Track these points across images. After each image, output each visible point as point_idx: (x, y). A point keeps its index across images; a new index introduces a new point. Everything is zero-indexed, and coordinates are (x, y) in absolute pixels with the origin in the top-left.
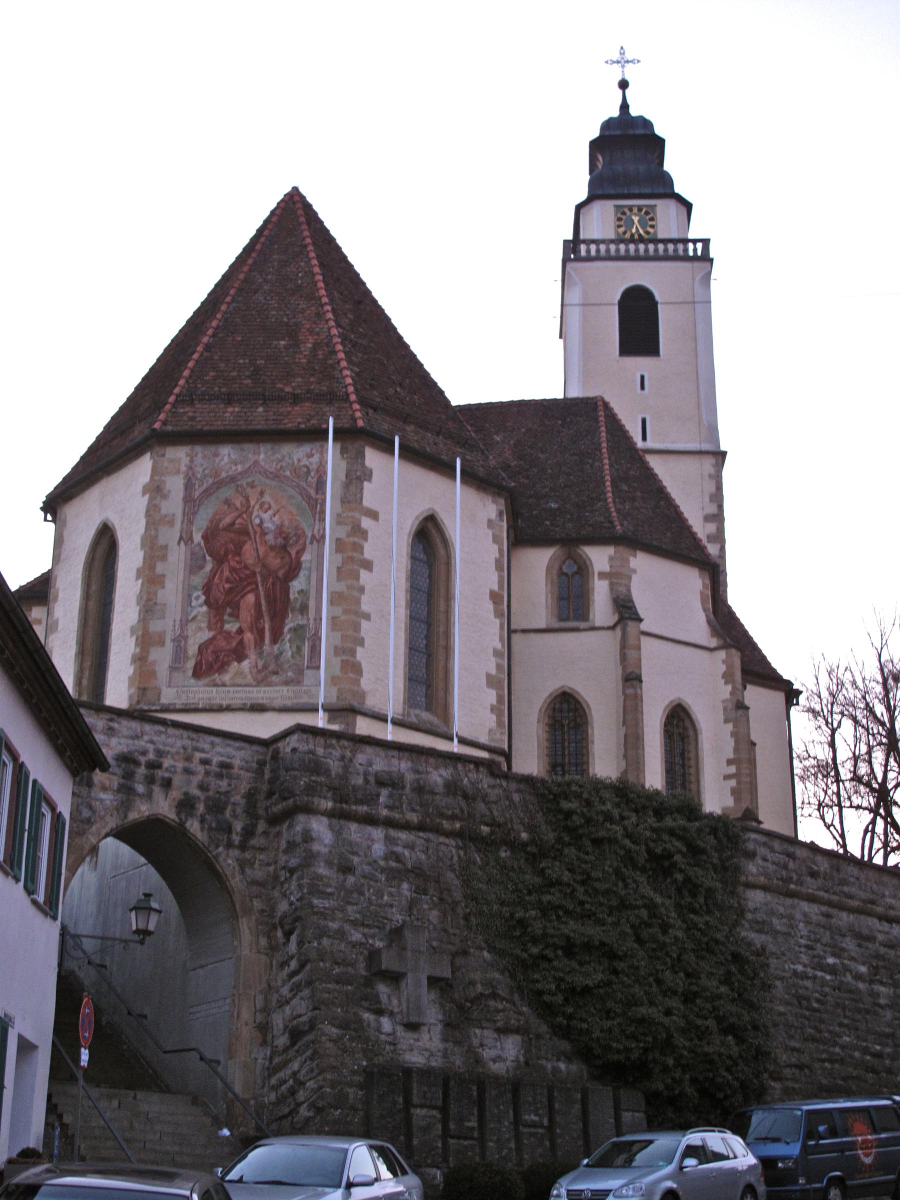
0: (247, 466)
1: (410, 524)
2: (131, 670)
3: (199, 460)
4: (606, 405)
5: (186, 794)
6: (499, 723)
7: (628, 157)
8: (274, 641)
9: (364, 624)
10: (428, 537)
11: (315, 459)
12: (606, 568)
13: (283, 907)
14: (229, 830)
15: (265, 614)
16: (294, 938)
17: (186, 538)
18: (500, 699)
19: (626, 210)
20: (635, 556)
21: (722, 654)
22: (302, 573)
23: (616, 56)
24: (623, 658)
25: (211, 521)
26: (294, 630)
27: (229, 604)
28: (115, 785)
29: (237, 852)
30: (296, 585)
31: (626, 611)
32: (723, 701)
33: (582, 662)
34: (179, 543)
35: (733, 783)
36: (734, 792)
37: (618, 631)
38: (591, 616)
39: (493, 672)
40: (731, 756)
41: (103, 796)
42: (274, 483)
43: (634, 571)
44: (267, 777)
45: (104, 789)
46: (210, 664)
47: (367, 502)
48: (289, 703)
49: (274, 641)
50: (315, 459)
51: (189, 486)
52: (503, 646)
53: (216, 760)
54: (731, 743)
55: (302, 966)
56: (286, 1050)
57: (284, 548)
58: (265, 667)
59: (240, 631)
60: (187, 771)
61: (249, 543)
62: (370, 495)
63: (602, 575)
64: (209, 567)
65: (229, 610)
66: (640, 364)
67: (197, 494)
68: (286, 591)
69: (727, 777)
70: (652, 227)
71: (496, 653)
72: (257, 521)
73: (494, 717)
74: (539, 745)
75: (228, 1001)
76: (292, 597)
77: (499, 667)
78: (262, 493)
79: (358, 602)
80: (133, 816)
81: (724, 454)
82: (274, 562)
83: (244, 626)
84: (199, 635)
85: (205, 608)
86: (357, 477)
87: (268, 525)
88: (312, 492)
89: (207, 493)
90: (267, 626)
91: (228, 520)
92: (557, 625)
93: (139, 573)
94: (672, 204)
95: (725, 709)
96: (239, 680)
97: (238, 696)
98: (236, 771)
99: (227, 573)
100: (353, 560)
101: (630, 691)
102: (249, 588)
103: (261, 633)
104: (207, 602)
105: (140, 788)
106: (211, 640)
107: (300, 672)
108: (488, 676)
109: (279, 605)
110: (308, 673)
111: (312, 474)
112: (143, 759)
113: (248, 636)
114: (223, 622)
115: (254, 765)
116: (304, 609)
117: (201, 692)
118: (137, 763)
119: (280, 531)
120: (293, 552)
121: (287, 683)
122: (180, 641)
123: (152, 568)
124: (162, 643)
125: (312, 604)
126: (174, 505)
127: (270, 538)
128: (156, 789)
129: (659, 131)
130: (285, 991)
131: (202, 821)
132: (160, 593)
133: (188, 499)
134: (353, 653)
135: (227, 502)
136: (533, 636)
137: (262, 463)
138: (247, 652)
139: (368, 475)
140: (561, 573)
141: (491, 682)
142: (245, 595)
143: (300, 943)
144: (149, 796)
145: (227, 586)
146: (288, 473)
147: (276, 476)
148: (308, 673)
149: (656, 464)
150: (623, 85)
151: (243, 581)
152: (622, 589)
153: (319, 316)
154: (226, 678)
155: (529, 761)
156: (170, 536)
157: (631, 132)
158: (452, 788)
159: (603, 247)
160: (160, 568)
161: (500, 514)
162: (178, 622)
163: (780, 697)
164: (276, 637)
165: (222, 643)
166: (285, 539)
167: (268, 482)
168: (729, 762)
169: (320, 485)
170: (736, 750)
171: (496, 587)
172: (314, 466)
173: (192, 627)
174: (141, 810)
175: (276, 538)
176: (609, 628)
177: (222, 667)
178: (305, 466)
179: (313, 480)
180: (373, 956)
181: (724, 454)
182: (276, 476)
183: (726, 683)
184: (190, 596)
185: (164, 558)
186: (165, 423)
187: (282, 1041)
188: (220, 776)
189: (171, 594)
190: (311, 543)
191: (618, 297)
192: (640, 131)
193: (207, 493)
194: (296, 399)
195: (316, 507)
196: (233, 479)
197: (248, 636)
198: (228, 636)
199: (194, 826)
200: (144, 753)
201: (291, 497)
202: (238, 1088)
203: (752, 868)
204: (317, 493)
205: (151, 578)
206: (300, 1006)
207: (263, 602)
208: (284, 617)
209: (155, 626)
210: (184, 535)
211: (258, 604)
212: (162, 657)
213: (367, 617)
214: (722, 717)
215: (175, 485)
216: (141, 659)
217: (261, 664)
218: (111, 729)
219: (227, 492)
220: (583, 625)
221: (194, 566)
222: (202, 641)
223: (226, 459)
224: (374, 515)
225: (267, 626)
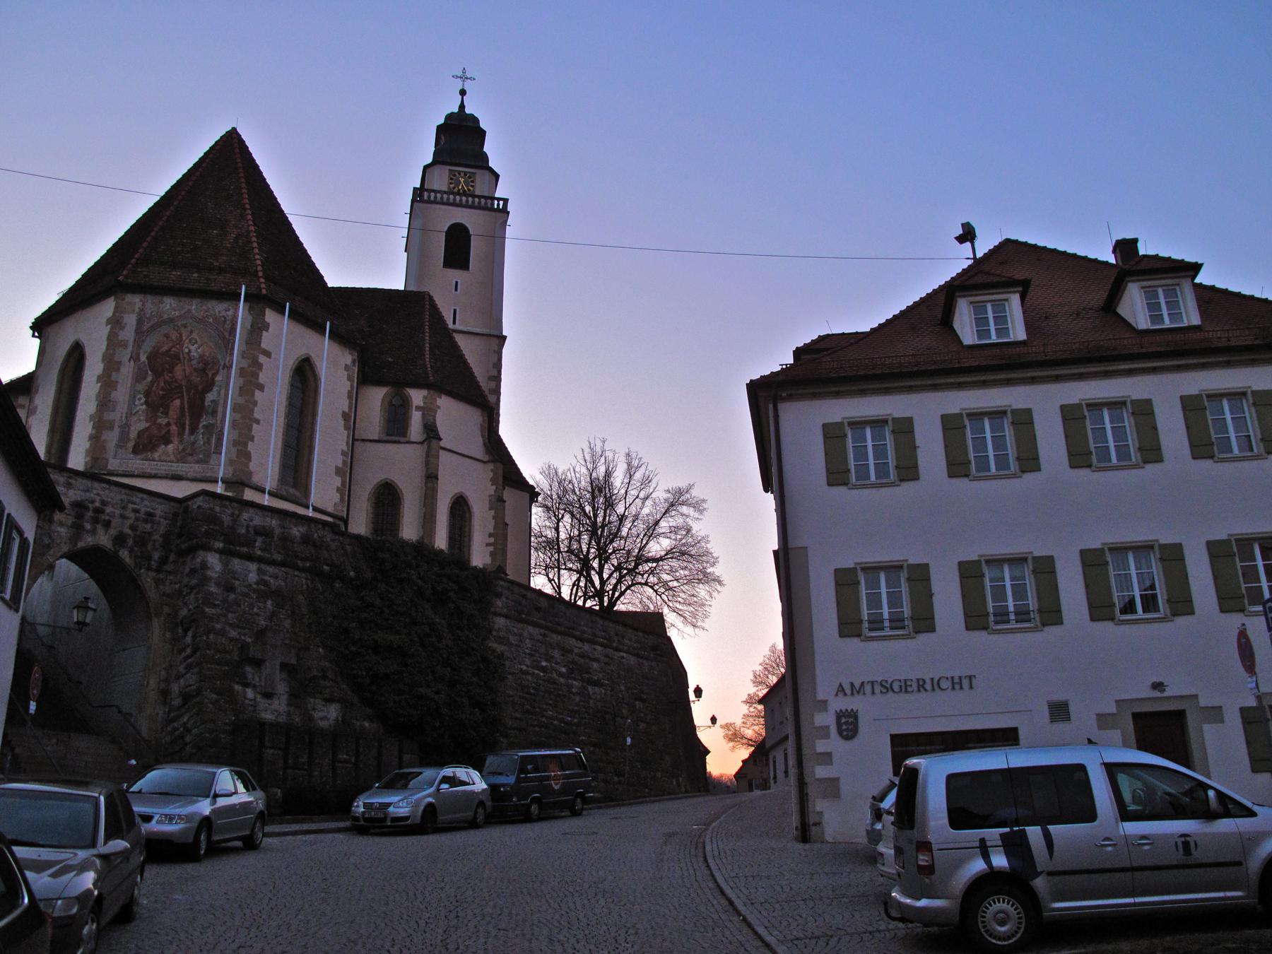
1: (291, 363)
2: (88, 445)
3: (149, 305)
4: (431, 298)
5: (121, 532)
6: (342, 500)
7: (460, 140)
8: (192, 431)
9: (255, 426)
10: (304, 373)
11: (230, 313)
12: (421, 404)
13: (184, 612)
14: (149, 558)
16: (190, 634)
17: (135, 358)
18: (343, 484)
21: (491, 466)
22: (215, 389)
23: (460, 74)
24: (427, 463)
28: (69, 522)
29: (154, 574)
30: (210, 397)
31: (431, 432)
33: (400, 464)
35: (491, 548)
36: (492, 554)
37: (425, 445)
41: (59, 529)
45: (61, 524)
46: (145, 445)
48: (198, 476)
49: (192, 431)
50: (230, 313)
51: (140, 322)
53: (143, 510)
54: (493, 522)
55: (194, 652)
56: (179, 708)
57: (204, 370)
58: (184, 450)
59: (168, 424)
60: (122, 516)
62: (267, 340)
63: (418, 408)
64: (149, 379)
66: (455, 275)
68: (203, 400)
69: (488, 545)
71: (344, 453)
77: (344, 463)
78: (191, 332)
79: (252, 411)
80: (81, 545)
81: (505, 338)
82: (196, 379)
84: (138, 425)
86: (258, 328)
87: (194, 354)
89: (153, 328)
91: (165, 348)
92: (386, 438)
93: (99, 379)
94: (487, 173)
96: (163, 457)
97: (163, 468)
99: (162, 384)
100: (251, 382)
103: (182, 427)
104: (146, 403)
105: (88, 526)
106: (147, 429)
107: (209, 456)
108: (337, 468)
110: (214, 456)
113: (174, 428)
114: (157, 417)
116: (214, 413)
117: (137, 464)
118: (87, 509)
119: (201, 356)
121: (197, 462)
122: (125, 427)
123: (109, 376)
124: (111, 428)
125: (220, 410)
126: (128, 334)
127: (194, 362)
128: (99, 527)
130: (182, 669)
131: (131, 551)
132: (113, 394)
133: (139, 331)
134: (246, 445)
135: (167, 336)
136: (368, 444)
139: (266, 327)
140: (391, 404)
141: (339, 472)
143: (194, 637)
144: (93, 532)
148: (214, 456)
149: (459, 339)
150: (463, 93)
151: (173, 390)
153: (243, 217)
154: (156, 455)
155: (360, 525)
156: (124, 355)
158: (306, 539)
159: (439, 196)
161: (354, 362)
163: (527, 496)
164: (193, 430)
168: (490, 535)
169: (233, 331)
173: (134, 419)
174: (88, 540)
177: (154, 448)
179: (227, 326)
180: (244, 647)
181: (505, 338)
185: (118, 370)
186: (126, 277)
188: (146, 521)
189: (121, 396)
191: (446, 229)
192: (470, 124)
193: (153, 328)
194: (221, 271)
195: (228, 345)
196: (171, 321)
197: (174, 428)
199: (124, 554)
200: (93, 502)
202: (144, 733)
203: (499, 603)
205: (107, 383)
206: (191, 679)
208: (200, 416)
209: (108, 416)
211: (182, 408)
212: (112, 437)
213: (258, 422)
215: (131, 320)
216: (95, 438)
217: (181, 447)
218: (70, 484)
219: (165, 329)
220: (402, 439)
221: (139, 377)
224: (268, 354)
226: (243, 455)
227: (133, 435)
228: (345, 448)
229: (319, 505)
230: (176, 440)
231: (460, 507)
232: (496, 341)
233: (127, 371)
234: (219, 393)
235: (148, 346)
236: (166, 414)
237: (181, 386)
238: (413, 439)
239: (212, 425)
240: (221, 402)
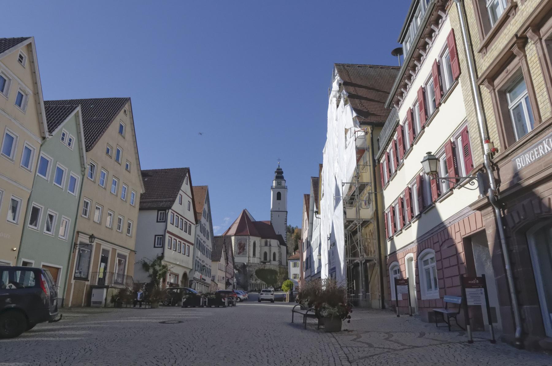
10: (254, 244)
31: (270, 245)
33: (266, 249)
46: (239, 254)
66: (279, 201)
86: (249, 239)
100: (249, 246)
109: (244, 249)
129: (283, 170)
226: (249, 254)
231: (274, 254)
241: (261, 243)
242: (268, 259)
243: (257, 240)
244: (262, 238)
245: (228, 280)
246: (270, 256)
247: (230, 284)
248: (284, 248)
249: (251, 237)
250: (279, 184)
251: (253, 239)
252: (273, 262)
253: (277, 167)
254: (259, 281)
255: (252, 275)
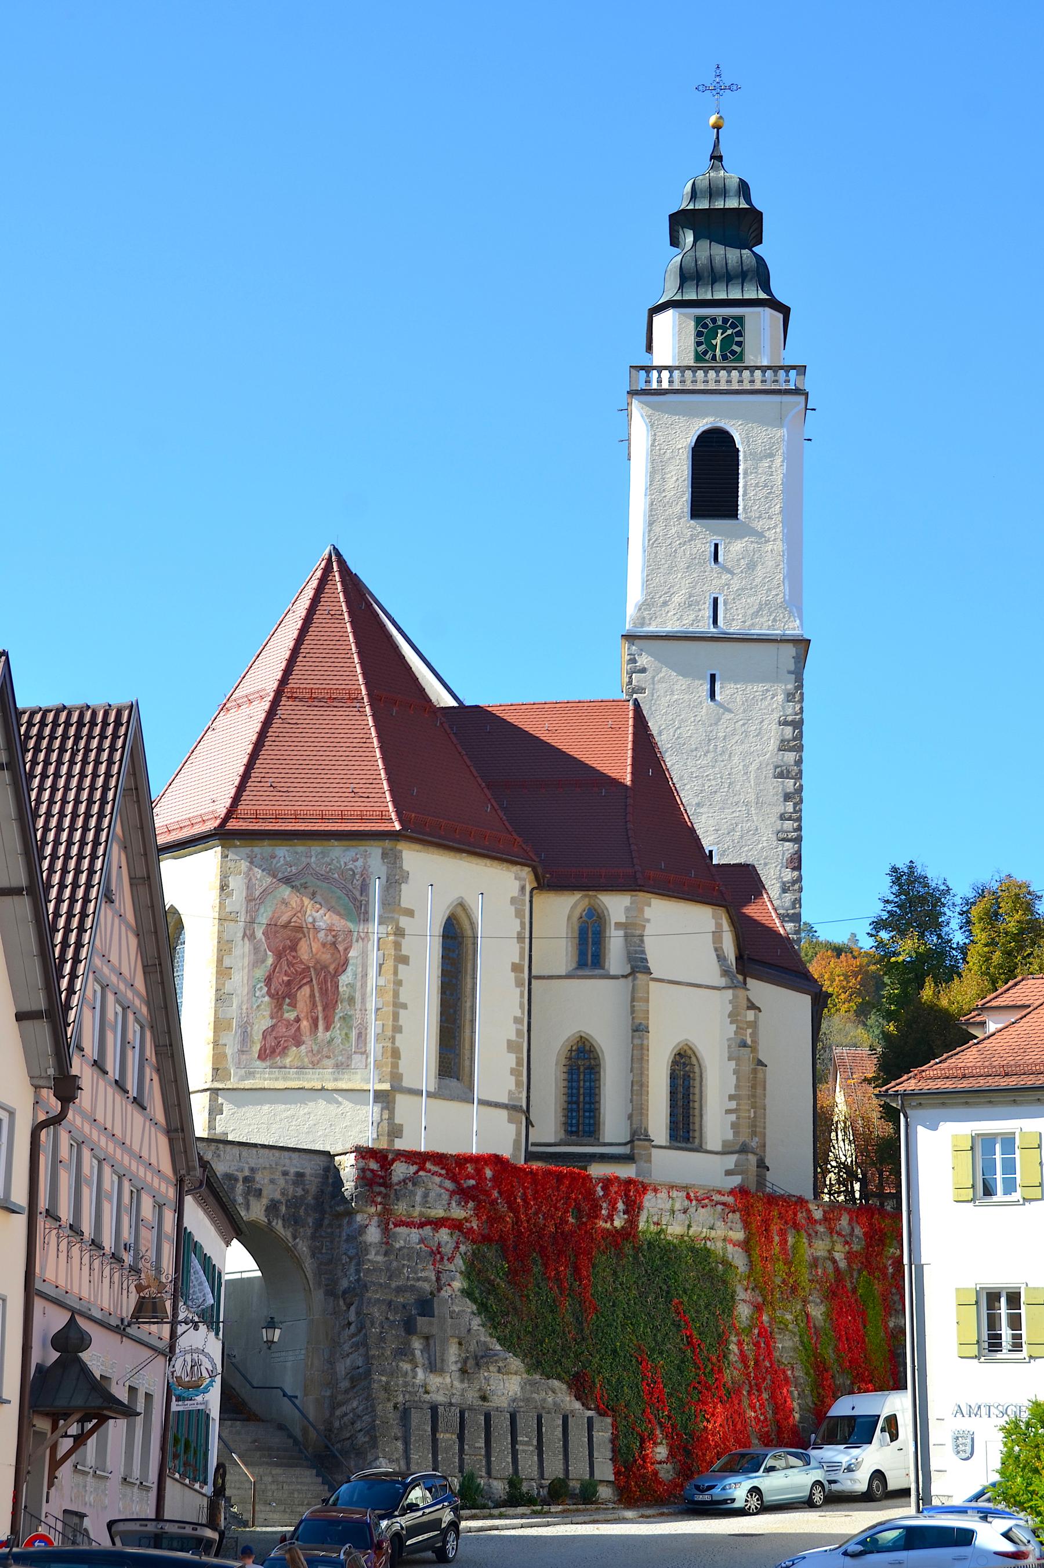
0: (300, 868)
6: (518, 1084)
8: (327, 1029)
10: (456, 941)
13: (344, 1284)
15: (319, 1004)
16: (353, 1309)
18: (519, 1063)
19: (708, 321)
20: (649, 905)
21: (729, 994)
22: (349, 968)
25: (271, 919)
26: (343, 1018)
27: (289, 995)
30: (344, 979)
31: (638, 965)
32: (729, 1040)
34: (243, 939)
36: (734, 1126)
37: (630, 978)
38: (607, 964)
39: (513, 1037)
40: (733, 1092)
42: (325, 885)
43: (648, 921)
44: (331, 1181)
47: (404, 904)
49: (327, 1029)
50: (360, 863)
52: (523, 1013)
53: (292, 1170)
54: (733, 1079)
56: (346, 1392)
57: (334, 944)
58: (318, 1052)
59: (298, 1020)
61: (304, 940)
62: (407, 896)
64: (270, 961)
65: (287, 1001)
67: (257, 893)
69: (728, 1112)
70: (740, 344)
71: (517, 1020)
72: (310, 920)
73: (513, 1078)
74: (556, 1085)
75: (303, 1352)
76: (340, 989)
77: (519, 1033)
83: (302, 1016)
84: (263, 1022)
85: (267, 999)
86: (395, 880)
88: (357, 894)
90: (320, 1016)
91: (284, 919)
94: (767, 314)
95: (729, 1047)
98: (308, 1178)
101: (637, 1041)
102: (305, 981)
104: (269, 993)
106: (273, 1027)
107: (349, 1058)
108: (509, 1043)
110: (356, 1058)
111: (357, 877)
112: (240, 1176)
113: (305, 1024)
115: (321, 1172)
116: (351, 1000)
118: (236, 1180)
120: (341, 948)
125: (358, 996)
130: (346, 1347)
133: (250, 899)
137: (314, 866)
138: (304, 1038)
141: (511, 1046)
142: (300, 988)
143: (358, 1313)
145: (286, 978)
146: (336, 875)
147: (325, 878)
148: (356, 1058)
152: (636, 940)
154: (288, 1061)
157: (719, 204)
160: (227, 962)
162: (244, 1011)
165: (282, 1030)
166: (334, 936)
167: (319, 883)
168: (731, 1098)
169: (364, 888)
170: (737, 1087)
171: (517, 961)
172: (359, 870)
175: (327, 936)
176: (623, 976)
177: (284, 1051)
178: (351, 869)
179: (357, 883)
182: (325, 878)
183: (731, 1023)
184: (255, 987)
187: (345, 1384)
190: (357, 941)
197: (305, 1024)
198: (289, 1024)
199: (278, 1226)
201: (340, 898)
202: (311, 1416)
204: (361, 895)
207: (317, 995)
210: (248, 932)
211: (312, 996)
214: (726, 1055)
217: (315, 1048)
220: (597, 972)
222: (264, 1028)
223: (282, 861)
224: (410, 913)
225: (320, 1016)
227: (257, 1037)
228: (519, 1014)
229: (485, 1097)
230: (306, 1038)
232: (790, 650)
233: (242, 950)
234: (355, 975)
235: (264, 919)
236: (293, 1005)
237: (309, 967)
238: (612, 972)
239: (350, 1016)
240: (359, 984)
241: (528, 938)
242: (613, 1126)
243: (491, 891)
244: (550, 880)
245: (70, 1341)
246: (638, 1087)
247: (100, 1405)
248: (785, 1009)
249: (415, 859)
250: (719, 343)
251: (438, 881)
252: (668, 1164)
253: (700, 170)
254: (508, 1385)
255: (426, 1306)
